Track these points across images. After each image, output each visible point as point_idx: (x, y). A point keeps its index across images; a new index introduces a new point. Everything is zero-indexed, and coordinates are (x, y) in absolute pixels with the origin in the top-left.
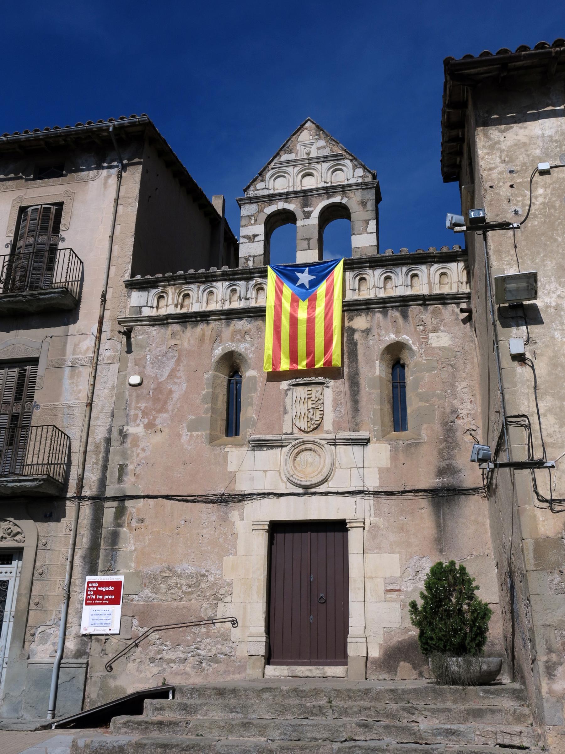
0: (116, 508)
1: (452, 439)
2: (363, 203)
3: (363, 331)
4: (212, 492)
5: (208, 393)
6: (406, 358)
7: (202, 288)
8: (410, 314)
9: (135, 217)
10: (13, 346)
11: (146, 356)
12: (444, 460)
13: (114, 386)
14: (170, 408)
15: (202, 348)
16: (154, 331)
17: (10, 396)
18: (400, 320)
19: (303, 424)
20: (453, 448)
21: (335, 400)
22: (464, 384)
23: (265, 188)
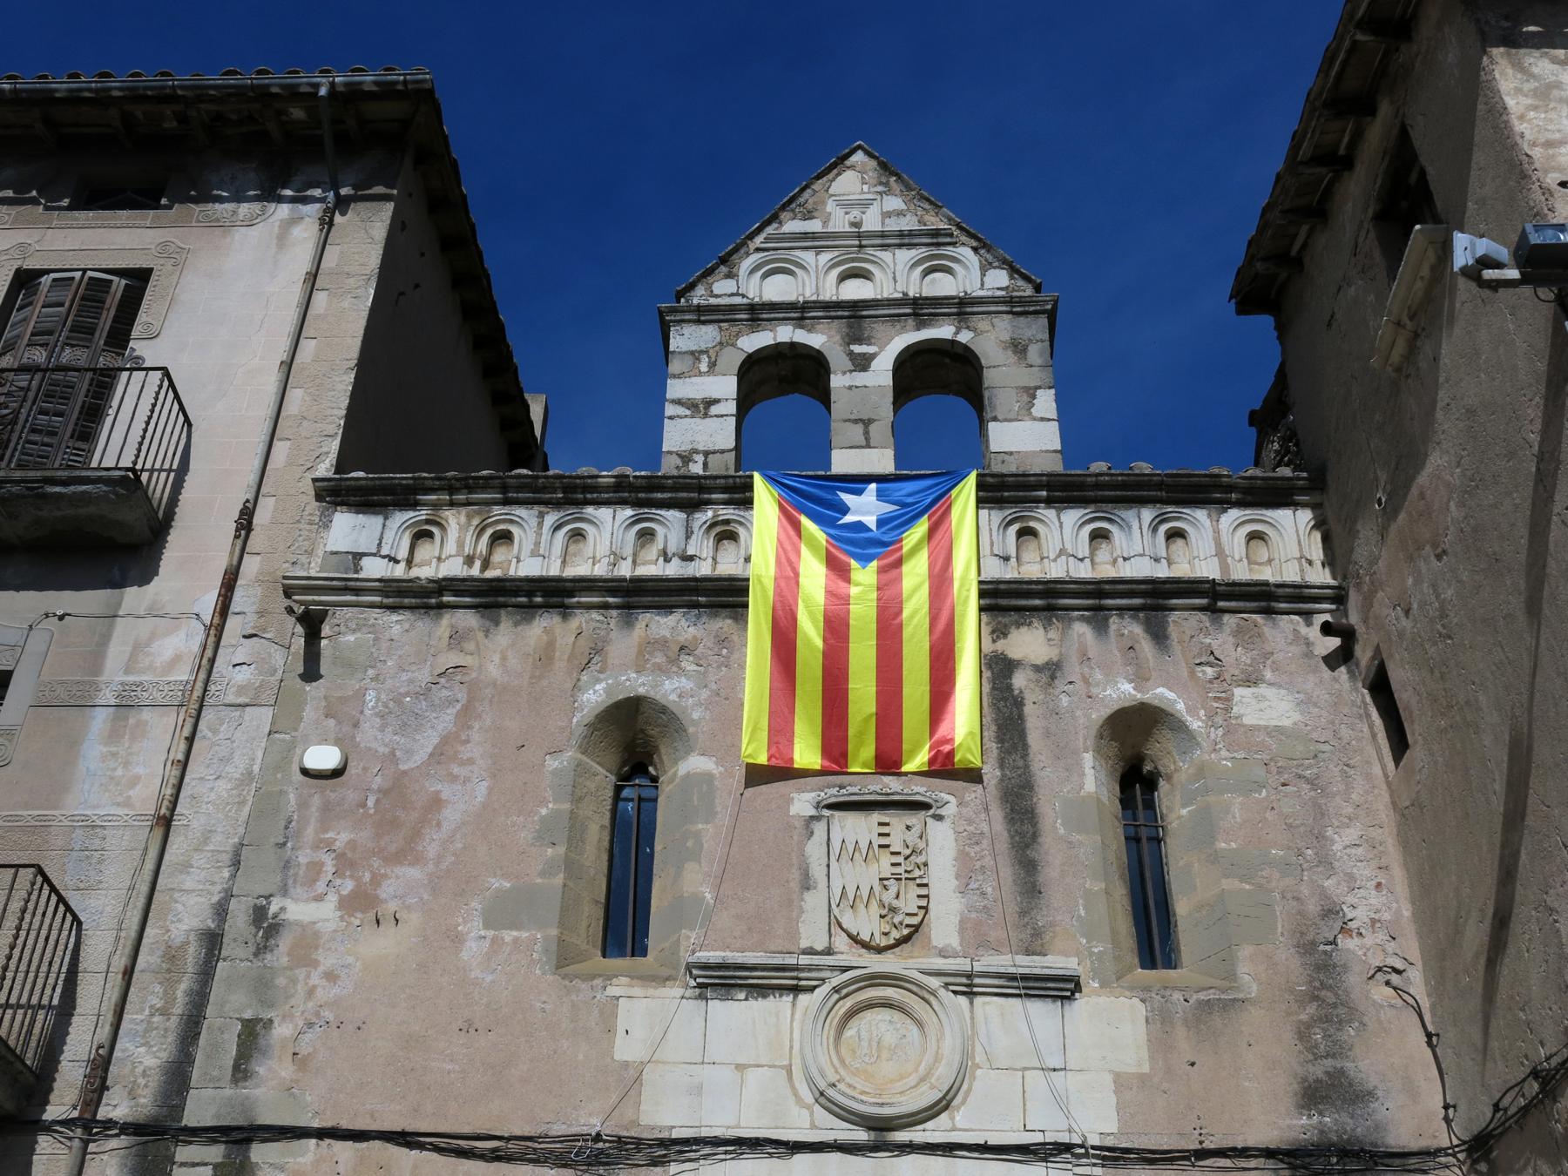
0: (216, 1166)
1: (1336, 994)
2: (1018, 348)
3: (1037, 669)
4: (559, 1129)
6: (1163, 753)
7: (551, 518)
8: (1172, 630)
11: (360, 695)
12: (1317, 1057)
13: (250, 773)
14: (432, 850)
15: (545, 683)
16: (396, 624)
18: (1146, 646)
19: (867, 924)
20: (1340, 1022)
21: (962, 858)
22: (1352, 834)
23: (737, 294)
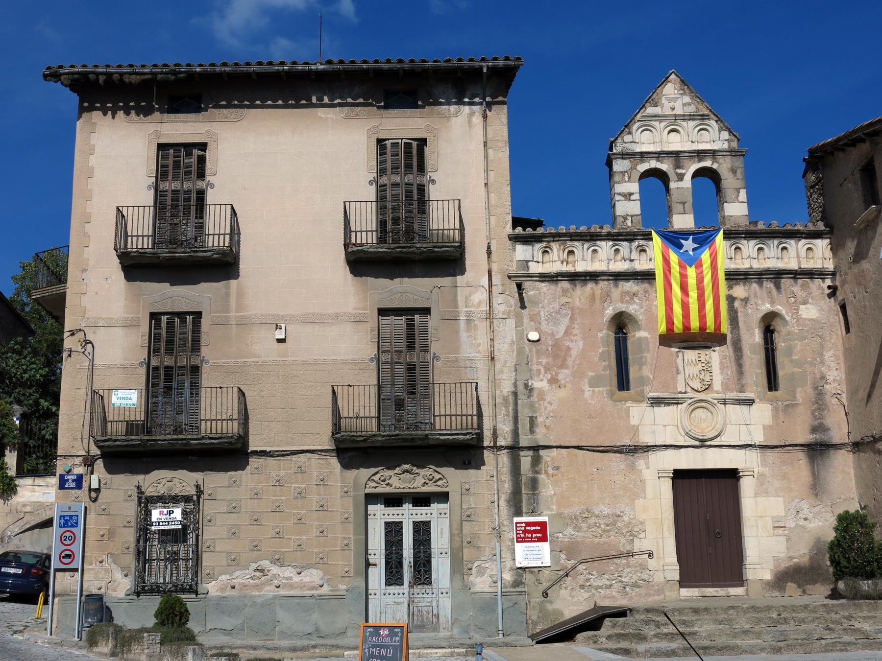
2: (733, 171)
3: (742, 300)
4: (618, 444)
5: (604, 351)
6: (777, 324)
7: (586, 246)
8: (782, 286)
9: (508, 163)
10: (399, 295)
11: (539, 312)
16: (544, 286)
17: (402, 345)
18: (774, 291)
19: (697, 385)
21: (721, 363)
22: (830, 353)
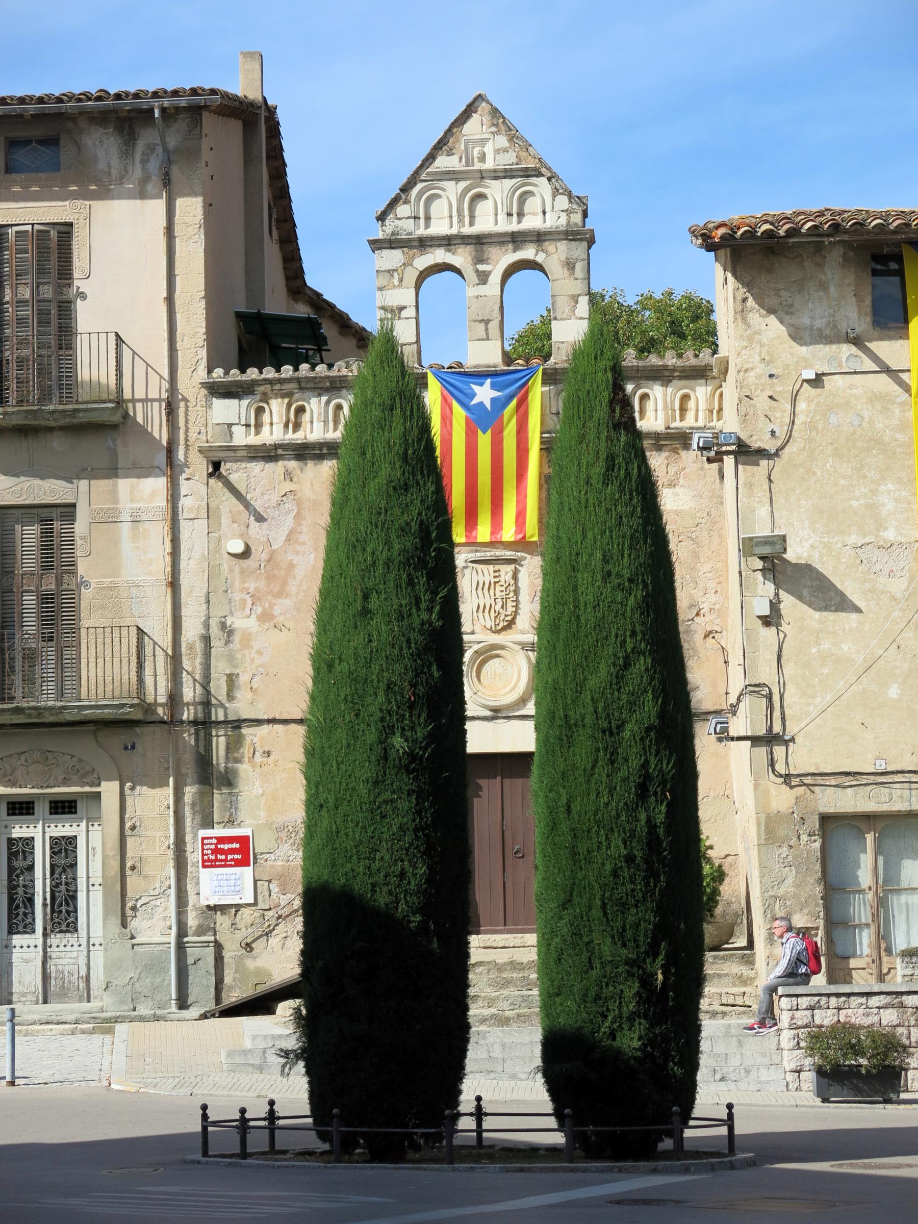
2: (570, 265)
7: (324, 399)
16: (256, 468)
